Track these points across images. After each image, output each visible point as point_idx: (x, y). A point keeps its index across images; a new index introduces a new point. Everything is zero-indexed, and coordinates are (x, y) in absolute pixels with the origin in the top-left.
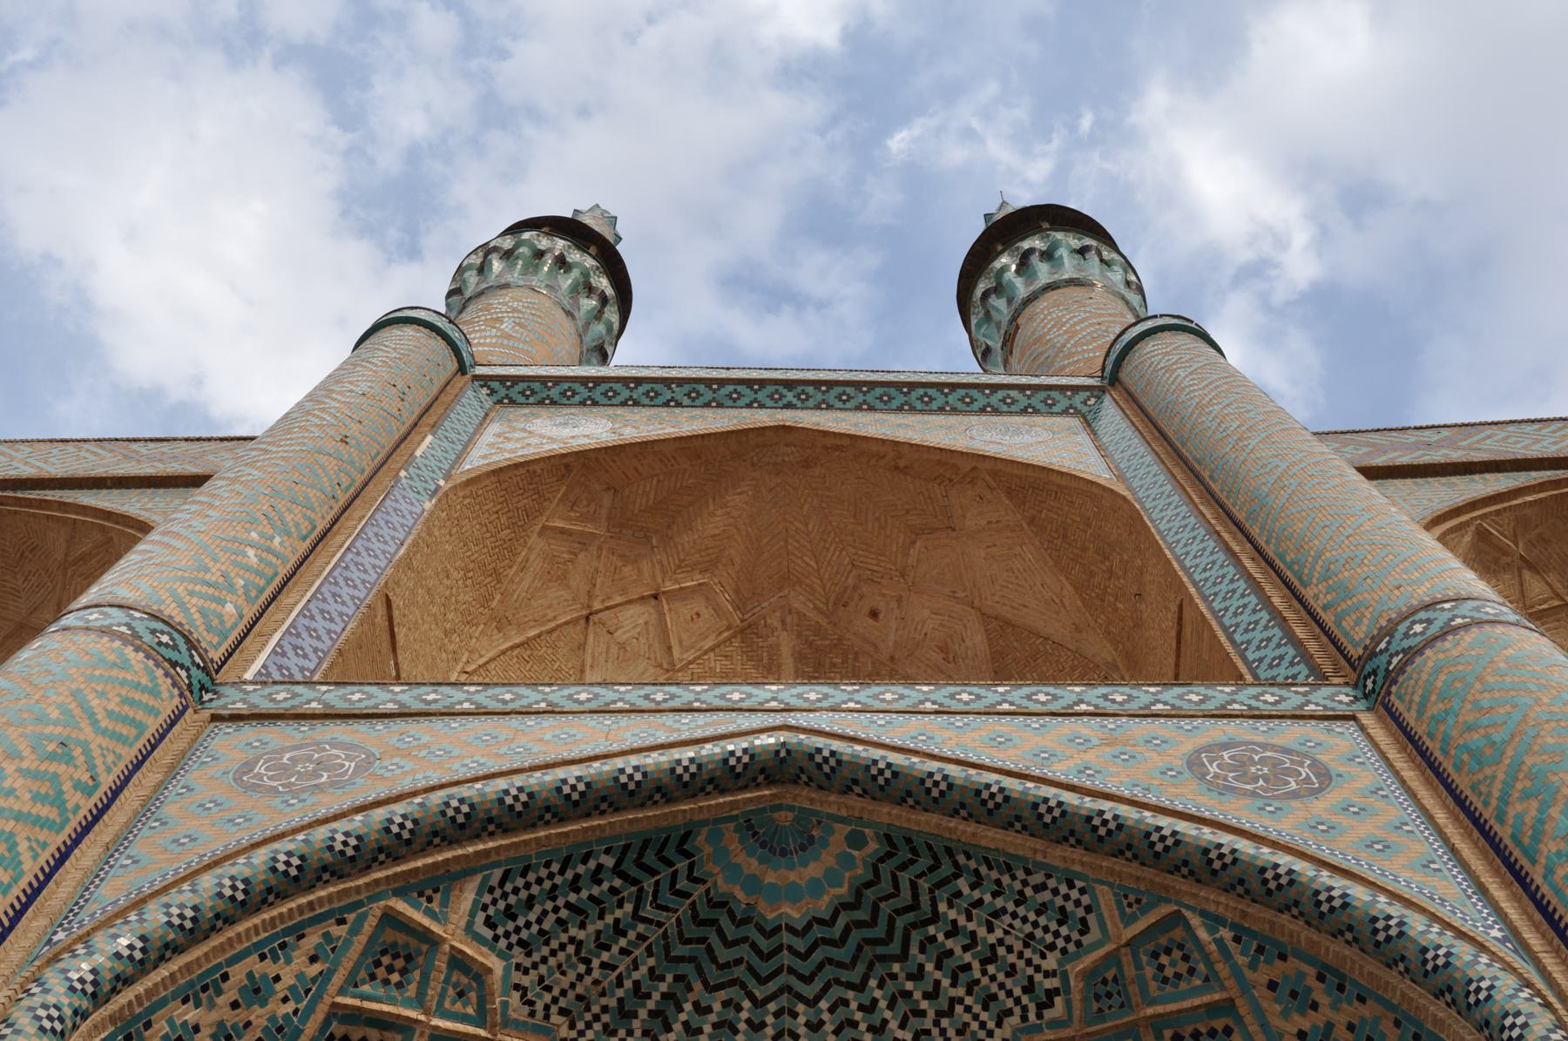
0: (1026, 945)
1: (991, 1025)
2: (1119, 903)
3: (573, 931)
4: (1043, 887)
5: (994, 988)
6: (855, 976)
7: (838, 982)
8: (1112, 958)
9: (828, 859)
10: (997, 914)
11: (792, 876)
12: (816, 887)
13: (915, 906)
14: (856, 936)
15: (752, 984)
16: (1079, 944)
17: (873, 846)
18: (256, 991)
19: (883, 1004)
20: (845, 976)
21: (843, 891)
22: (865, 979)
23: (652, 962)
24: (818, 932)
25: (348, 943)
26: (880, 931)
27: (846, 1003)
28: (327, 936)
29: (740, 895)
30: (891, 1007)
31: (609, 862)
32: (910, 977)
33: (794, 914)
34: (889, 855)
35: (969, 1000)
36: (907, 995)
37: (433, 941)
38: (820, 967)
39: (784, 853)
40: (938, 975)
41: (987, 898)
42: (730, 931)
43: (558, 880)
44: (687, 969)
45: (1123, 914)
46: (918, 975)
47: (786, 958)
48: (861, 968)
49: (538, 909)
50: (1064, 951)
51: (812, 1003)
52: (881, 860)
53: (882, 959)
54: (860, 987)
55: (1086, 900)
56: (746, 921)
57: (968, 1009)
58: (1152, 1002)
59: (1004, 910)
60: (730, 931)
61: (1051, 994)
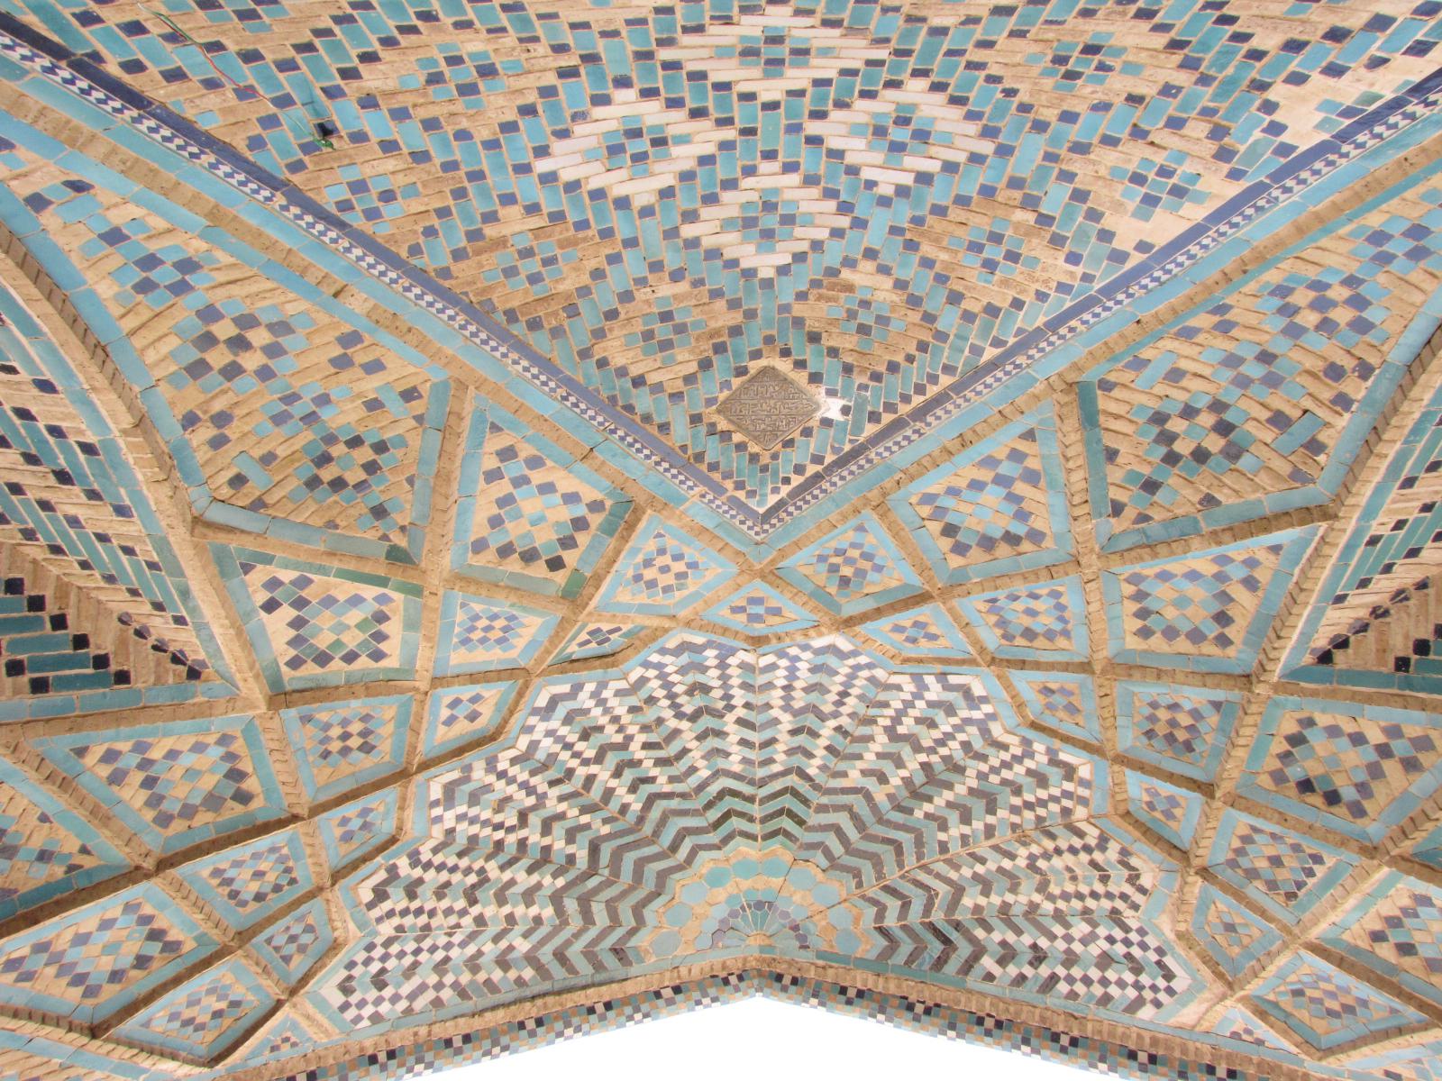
3: (1048, 907)
4: (412, 997)
5: (464, 863)
6: (662, 805)
13: (585, 902)
15: (803, 787)
31: (988, 963)
43: (1061, 971)
49: (1095, 950)
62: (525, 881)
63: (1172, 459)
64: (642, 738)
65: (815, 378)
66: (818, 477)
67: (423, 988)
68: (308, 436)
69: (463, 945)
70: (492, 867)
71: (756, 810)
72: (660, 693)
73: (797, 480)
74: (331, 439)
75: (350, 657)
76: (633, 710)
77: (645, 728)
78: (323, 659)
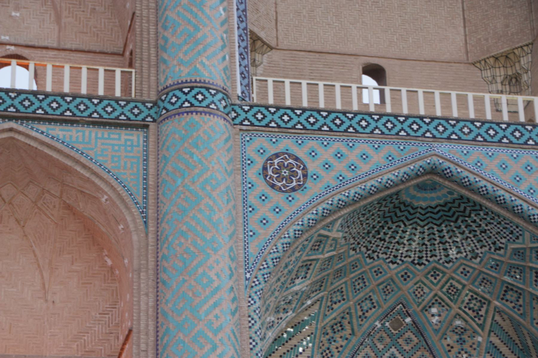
0: (497, 234)
1: (478, 247)
2: (531, 238)
4: (508, 224)
5: (482, 239)
6: (438, 223)
7: (432, 223)
8: (525, 249)
9: (439, 194)
10: (490, 223)
11: (426, 195)
12: (432, 199)
13: (464, 211)
14: (441, 213)
16: (514, 241)
17: (455, 196)
18: (286, 266)
19: (445, 231)
20: (435, 222)
21: (442, 202)
22: (441, 224)
23: (379, 219)
24: (429, 209)
25: (308, 245)
26: (450, 214)
27: (433, 228)
28: (303, 245)
29: (408, 200)
30: (448, 232)
32: (456, 227)
33: (424, 204)
34: (460, 199)
35: (473, 239)
36: (454, 231)
37: (327, 237)
38: (428, 218)
39: (425, 190)
40: (465, 229)
41: (488, 219)
42: (403, 208)
44: (388, 219)
45: (531, 240)
46: (459, 227)
47: (418, 215)
48: (441, 221)
50: (509, 240)
51: (423, 227)
52: (457, 199)
53: (448, 220)
54: (439, 226)
55: (520, 232)
56: (408, 206)
57: (472, 241)
58: (532, 263)
59: (493, 223)
60: (403, 208)
61: (500, 248)
62: (474, 225)
63: (340, 323)
64: (436, 242)
65: (389, 329)
66: (391, 312)
67: (505, 223)
68: (462, 337)
69: (493, 223)
70: (478, 233)
71: (418, 215)
72: (429, 252)
73: (394, 311)
74: (460, 335)
75: (476, 299)
76: (435, 250)
77: (434, 244)
78: (480, 301)
